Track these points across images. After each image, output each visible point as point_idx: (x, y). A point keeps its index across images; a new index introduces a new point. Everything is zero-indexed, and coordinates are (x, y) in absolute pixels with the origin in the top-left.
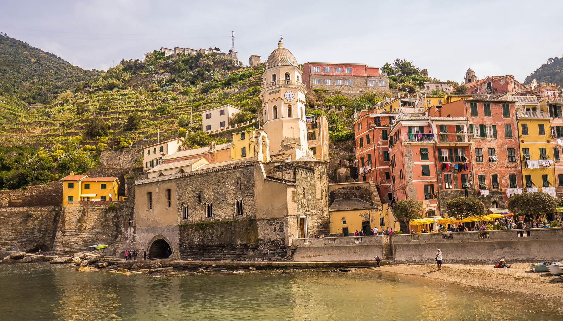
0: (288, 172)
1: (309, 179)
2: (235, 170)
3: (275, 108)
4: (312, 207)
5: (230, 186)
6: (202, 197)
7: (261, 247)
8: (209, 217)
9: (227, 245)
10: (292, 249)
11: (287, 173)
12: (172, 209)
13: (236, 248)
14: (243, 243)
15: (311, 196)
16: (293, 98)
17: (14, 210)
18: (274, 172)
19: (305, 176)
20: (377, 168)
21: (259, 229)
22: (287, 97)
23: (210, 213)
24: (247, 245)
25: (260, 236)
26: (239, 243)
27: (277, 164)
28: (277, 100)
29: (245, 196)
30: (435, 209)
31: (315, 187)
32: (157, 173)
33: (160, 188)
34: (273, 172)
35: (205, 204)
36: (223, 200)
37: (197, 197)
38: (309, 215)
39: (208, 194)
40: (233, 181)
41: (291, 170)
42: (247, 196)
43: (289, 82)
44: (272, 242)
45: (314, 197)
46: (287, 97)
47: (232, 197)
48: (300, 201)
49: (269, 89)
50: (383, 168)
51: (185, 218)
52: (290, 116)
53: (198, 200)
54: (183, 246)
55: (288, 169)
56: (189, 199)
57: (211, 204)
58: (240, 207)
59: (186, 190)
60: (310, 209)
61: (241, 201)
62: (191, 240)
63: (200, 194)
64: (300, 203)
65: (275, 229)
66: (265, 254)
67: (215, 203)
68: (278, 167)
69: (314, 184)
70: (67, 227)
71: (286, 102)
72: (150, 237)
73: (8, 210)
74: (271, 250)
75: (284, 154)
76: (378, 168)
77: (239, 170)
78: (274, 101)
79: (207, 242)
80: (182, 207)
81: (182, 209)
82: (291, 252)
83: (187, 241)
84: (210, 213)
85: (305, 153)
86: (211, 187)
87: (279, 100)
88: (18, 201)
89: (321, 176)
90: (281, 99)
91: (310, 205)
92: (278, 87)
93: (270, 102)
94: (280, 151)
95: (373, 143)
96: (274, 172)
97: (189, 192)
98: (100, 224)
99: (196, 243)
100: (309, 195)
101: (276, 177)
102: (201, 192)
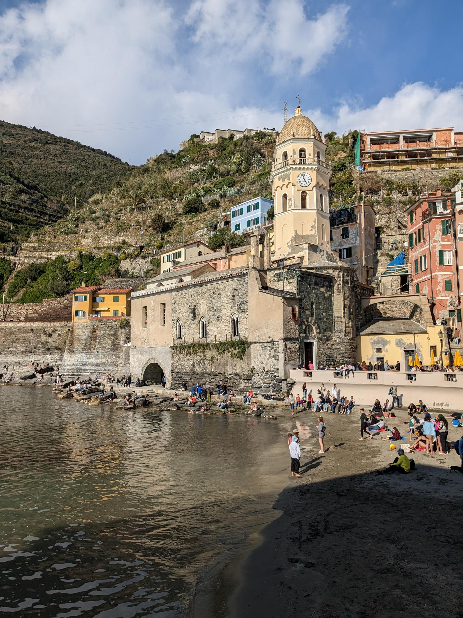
0: (290, 281)
1: (322, 290)
2: (231, 279)
4: (326, 328)
5: (225, 299)
6: (197, 312)
7: (254, 379)
9: (219, 373)
10: (289, 383)
11: (289, 283)
13: (227, 378)
14: (235, 372)
15: (324, 314)
16: (309, 182)
17: (28, 324)
18: (274, 281)
20: (433, 274)
21: (252, 355)
22: (300, 182)
23: (204, 334)
24: (239, 375)
25: (254, 364)
26: (231, 372)
29: (241, 312)
31: (331, 302)
32: (157, 284)
33: (155, 300)
34: (273, 282)
35: (200, 321)
36: (218, 317)
38: (321, 339)
40: (229, 294)
41: (293, 278)
42: (243, 312)
43: (304, 160)
45: (329, 315)
46: (300, 182)
47: (228, 313)
48: (305, 320)
50: (442, 275)
52: (304, 206)
55: (290, 277)
56: (183, 314)
57: (206, 322)
59: (181, 304)
60: (322, 331)
63: (194, 309)
64: (306, 323)
67: (209, 320)
68: (278, 275)
69: (331, 296)
70: (76, 346)
73: (23, 324)
74: (266, 383)
75: (293, 258)
77: (235, 279)
80: (176, 324)
81: (176, 327)
82: (287, 387)
83: (178, 366)
84: (204, 334)
85: (325, 256)
86: (207, 300)
87: (290, 185)
88: (33, 315)
89: (343, 287)
91: (323, 326)
92: (288, 168)
94: (289, 254)
95: (428, 239)
96: (274, 281)
97: (184, 308)
98: (111, 343)
101: (276, 288)
102: (195, 306)
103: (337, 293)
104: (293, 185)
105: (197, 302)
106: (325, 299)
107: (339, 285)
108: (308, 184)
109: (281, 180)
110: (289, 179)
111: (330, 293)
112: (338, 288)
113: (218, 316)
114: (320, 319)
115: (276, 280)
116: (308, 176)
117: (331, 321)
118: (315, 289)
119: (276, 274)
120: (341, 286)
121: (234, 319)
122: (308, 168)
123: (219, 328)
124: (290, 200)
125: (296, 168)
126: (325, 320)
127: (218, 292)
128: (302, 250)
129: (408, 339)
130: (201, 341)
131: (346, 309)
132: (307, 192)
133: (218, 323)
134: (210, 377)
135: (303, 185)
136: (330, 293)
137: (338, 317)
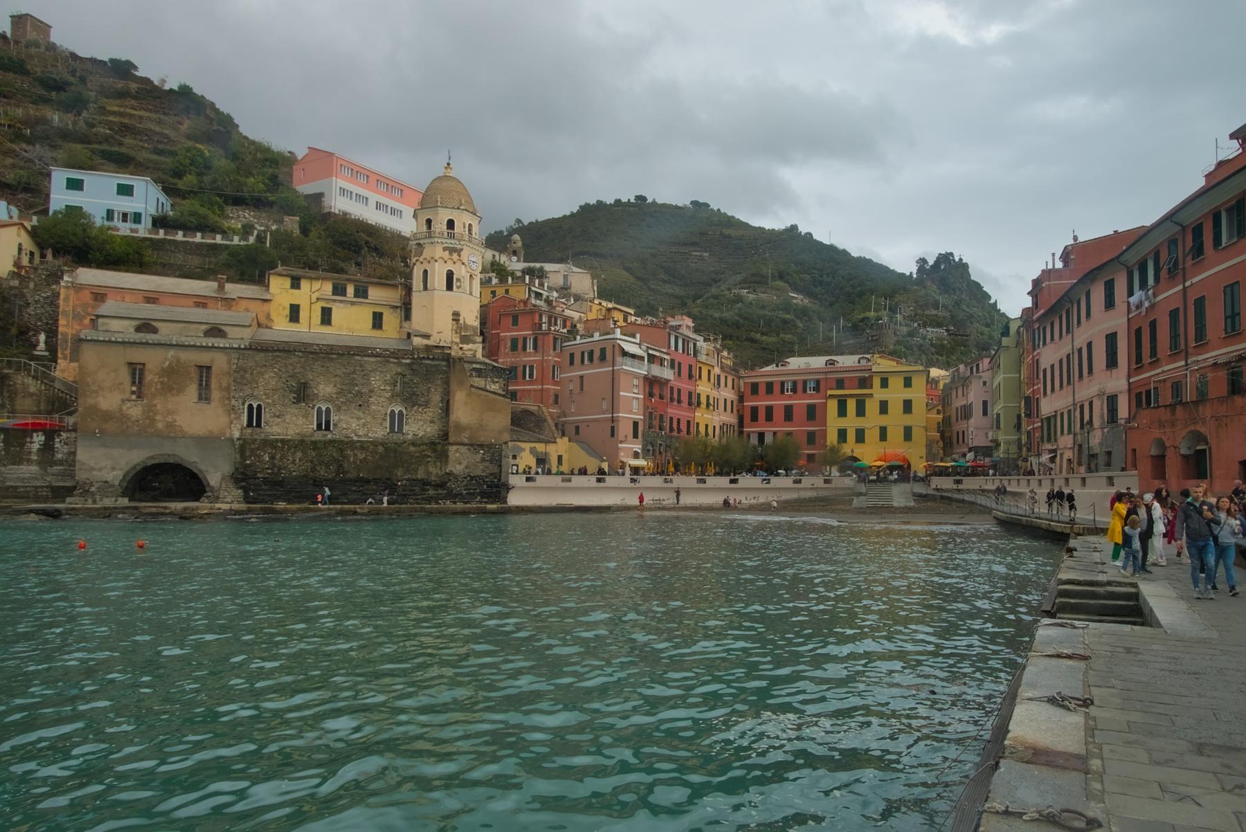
0: (496, 380)
2: (396, 361)
3: (450, 275)
8: (319, 427)
12: (213, 404)
20: (545, 387)
27: (478, 366)
28: (454, 263)
30: (639, 451)
35: (314, 406)
36: (360, 405)
37: (295, 393)
39: (324, 388)
40: (388, 377)
44: (472, 478)
49: (444, 241)
51: (250, 424)
53: (294, 398)
54: (258, 478)
58: (397, 421)
59: (262, 374)
61: (400, 412)
62: (279, 469)
65: (483, 460)
66: (456, 496)
71: (469, 270)
72: (137, 457)
76: (545, 387)
77: (404, 361)
78: (450, 262)
79: (326, 472)
80: (243, 404)
81: (243, 409)
90: (463, 264)
93: (440, 261)
99: (294, 474)
104: (463, 264)
105: (311, 377)
109: (447, 252)
110: (459, 255)
113: (361, 403)
115: (474, 374)
119: (474, 369)
121: (393, 412)
123: (363, 421)
124: (458, 280)
127: (363, 373)
128: (474, 342)
129: (540, 447)
130: (319, 436)
133: (360, 414)
134: (358, 484)
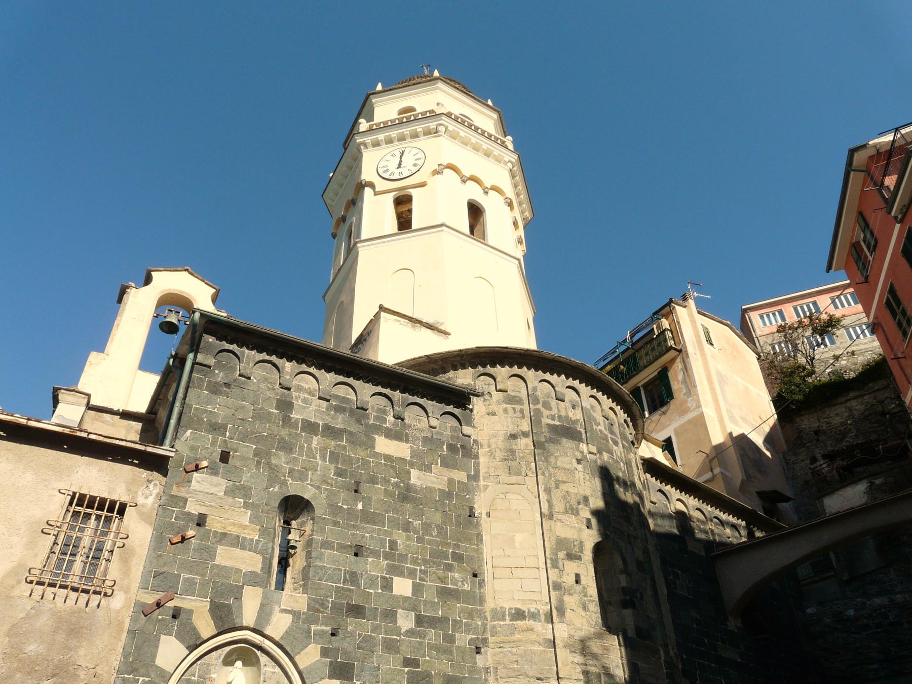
15: (402, 587)
19: (339, 422)
22: (387, 170)
45: (447, 594)
64: (205, 625)
100: (374, 567)
103: (505, 478)
106: (407, 495)
107: (514, 436)
108: (415, 169)
111: (460, 476)
112: (511, 454)
114: (357, 611)
116: (417, 151)
117: (463, 639)
118: (330, 432)
120: (525, 443)
122: (415, 136)
125: (376, 144)
126: (406, 621)
131: (571, 568)
132: (413, 192)
135: (396, 177)
136: (460, 476)
137: (519, 615)
